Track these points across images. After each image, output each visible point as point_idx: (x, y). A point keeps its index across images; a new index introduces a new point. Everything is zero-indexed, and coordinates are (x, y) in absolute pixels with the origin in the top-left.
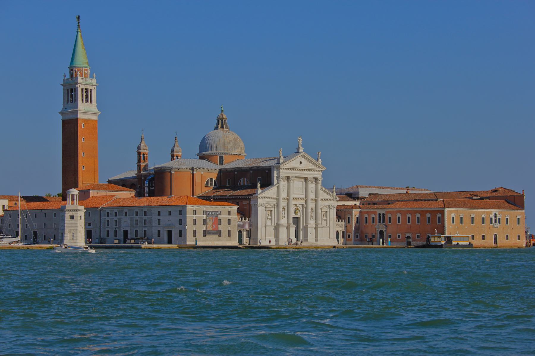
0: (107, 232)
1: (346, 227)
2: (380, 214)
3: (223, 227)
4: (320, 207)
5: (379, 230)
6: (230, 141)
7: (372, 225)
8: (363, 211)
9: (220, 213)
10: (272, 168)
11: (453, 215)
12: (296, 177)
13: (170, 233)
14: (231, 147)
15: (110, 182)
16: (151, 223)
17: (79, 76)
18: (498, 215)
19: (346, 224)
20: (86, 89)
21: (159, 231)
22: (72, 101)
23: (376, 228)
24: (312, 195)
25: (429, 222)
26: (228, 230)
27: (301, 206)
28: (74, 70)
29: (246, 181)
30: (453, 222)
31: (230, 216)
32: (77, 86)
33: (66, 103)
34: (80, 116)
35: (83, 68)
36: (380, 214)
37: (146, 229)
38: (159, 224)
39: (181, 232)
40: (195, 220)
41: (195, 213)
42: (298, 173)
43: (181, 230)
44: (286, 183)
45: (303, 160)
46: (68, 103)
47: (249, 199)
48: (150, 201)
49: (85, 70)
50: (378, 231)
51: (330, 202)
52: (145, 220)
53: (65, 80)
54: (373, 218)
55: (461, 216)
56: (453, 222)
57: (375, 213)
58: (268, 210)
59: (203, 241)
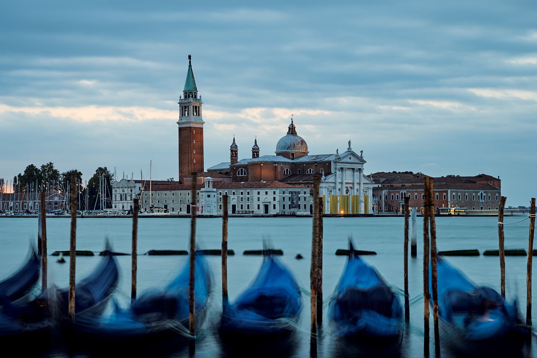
0: (248, 206)
1: (378, 202)
2: (402, 193)
3: (301, 203)
4: (362, 188)
5: (402, 204)
6: (299, 143)
7: (396, 201)
8: (390, 191)
9: (299, 193)
10: (332, 162)
11: (454, 194)
13: (266, 207)
15: (208, 170)
16: (253, 200)
17: (191, 97)
18: (483, 194)
19: (379, 200)
20: (195, 106)
21: (259, 205)
22: (185, 115)
23: (399, 203)
24: (357, 181)
25: (437, 199)
26: (305, 204)
27: (350, 188)
28: (187, 93)
29: (312, 171)
31: (306, 195)
32: (189, 104)
33: (181, 116)
34: (192, 125)
35: (194, 92)
36: (402, 193)
37: (249, 204)
38: (259, 200)
39: (275, 206)
40: (284, 198)
41: (284, 193)
42: (349, 166)
43: (275, 205)
44: (340, 172)
45: (351, 157)
46: (183, 116)
48: (251, 185)
49: (195, 93)
50: (401, 204)
51: (368, 185)
52: (248, 198)
53: (181, 99)
54: (398, 196)
55: (459, 194)
57: (399, 192)
58: (330, 191)
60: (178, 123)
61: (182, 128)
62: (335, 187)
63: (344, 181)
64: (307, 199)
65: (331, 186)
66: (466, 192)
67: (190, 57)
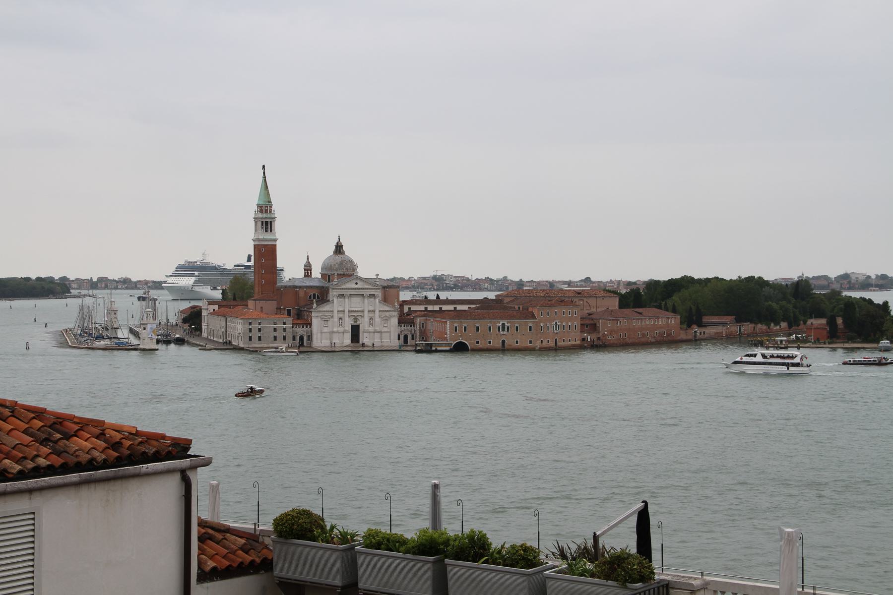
6: (337, 263)
11: (456, 325)
12: (350, 294)
14: (336, 268)
18: (506, 324)
20: (265, 222)
26: (284, 336)
27: (360, 317)
30: (456, 330)
35: (264, 206)
41: (250, 324)
42: (353, 292)
47: (311, 312)
49: (265, 207)
56: (456, 330)
59: (259, 344)
60: (254, 240)
61: (256, 245)
62: (333, 316)
63: (347, 311)
64: (287, 330)
65: (327, 315)
66: (477, 323)
67: (264, 167)
